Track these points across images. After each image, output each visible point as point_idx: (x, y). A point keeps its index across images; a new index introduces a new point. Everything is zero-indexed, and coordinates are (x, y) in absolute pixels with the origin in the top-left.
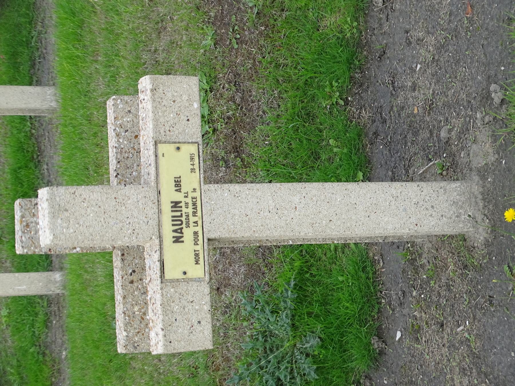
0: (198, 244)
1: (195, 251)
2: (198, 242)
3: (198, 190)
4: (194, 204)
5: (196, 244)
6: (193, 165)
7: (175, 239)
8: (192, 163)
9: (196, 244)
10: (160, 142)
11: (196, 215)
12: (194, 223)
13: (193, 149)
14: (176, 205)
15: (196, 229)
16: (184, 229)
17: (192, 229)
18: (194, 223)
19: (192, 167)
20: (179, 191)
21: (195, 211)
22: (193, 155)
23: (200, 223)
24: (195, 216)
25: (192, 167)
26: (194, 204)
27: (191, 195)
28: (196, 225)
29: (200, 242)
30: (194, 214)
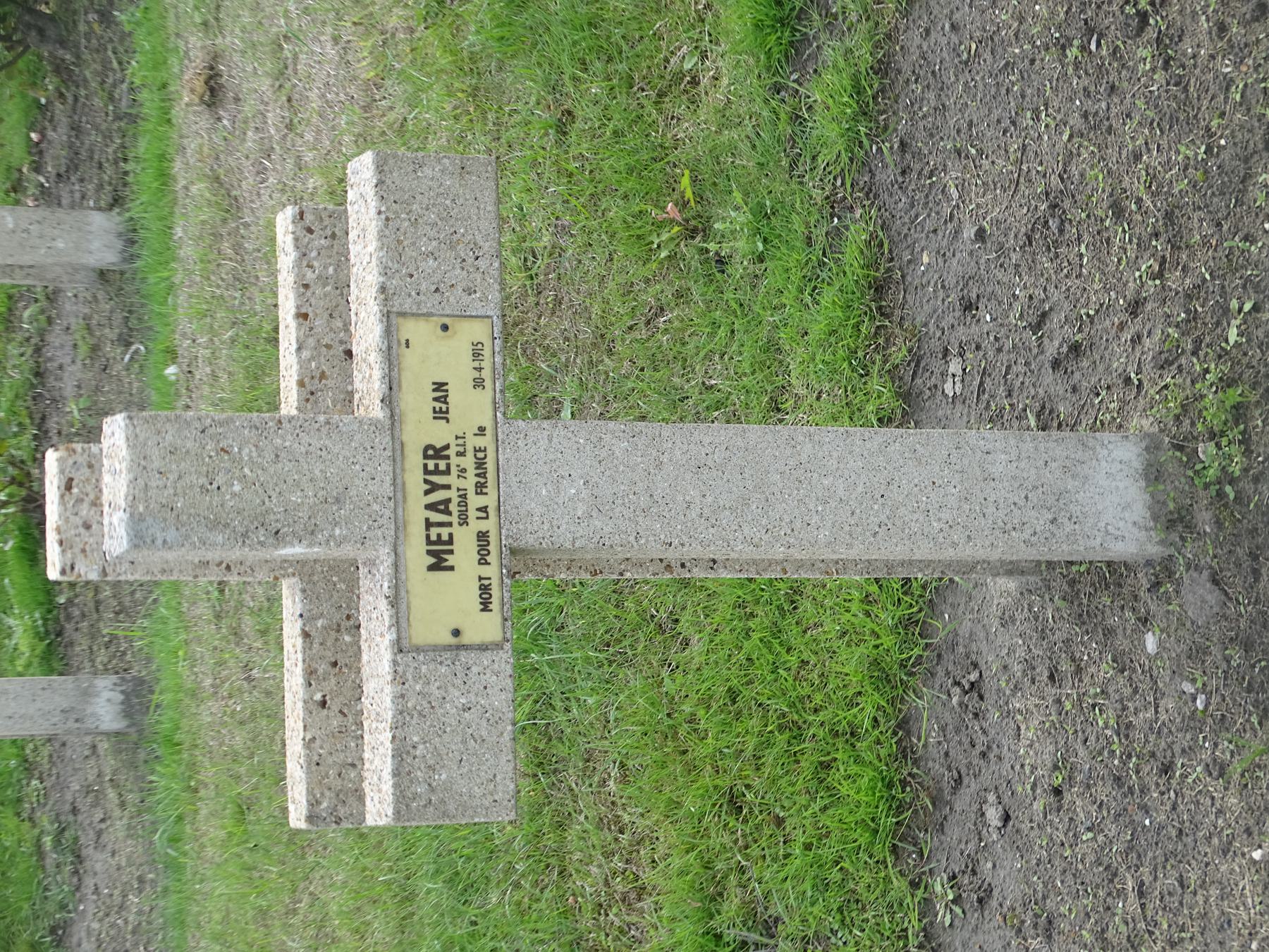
0: (487, 563)
1: (480, 578)
4: (480, 464)
8: (476, 364)
9: (483, 561)
10: (403, 314)
11: (485, 490)
12: (478, 509)
15: (483, 526)
16: (455, 524)
17: (476, 525)
18: (478, 509)
19: (477, 375)
21: (483, 480)
22: (480, 346)
23: (492, 511)
24: (482, 493)
25: (477, 375)
26: (480, 464)
27: (473, 442)
28: (484, 515)
30: (480, 488)
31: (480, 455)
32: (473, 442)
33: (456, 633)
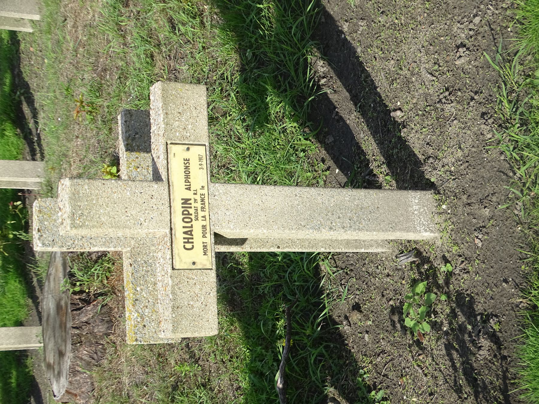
1: (203, 243)
3: (206, 188)
4: (203, 200)
6: (201, 165)
8: (200, 163)
9: (204, 236)
12: (202, 217)
13: (201, 151)
14: (186, 201)
15: (204, 223)
16: (194, 223)
18: (202, 217)
19: (201, 167)
20: (189, 189)
25: (201, 167)
26: (203, 200)
27: (200, 192)
30: (203, 209)
31: (203, 197)
32: (200, 192)
33: (194, 263)
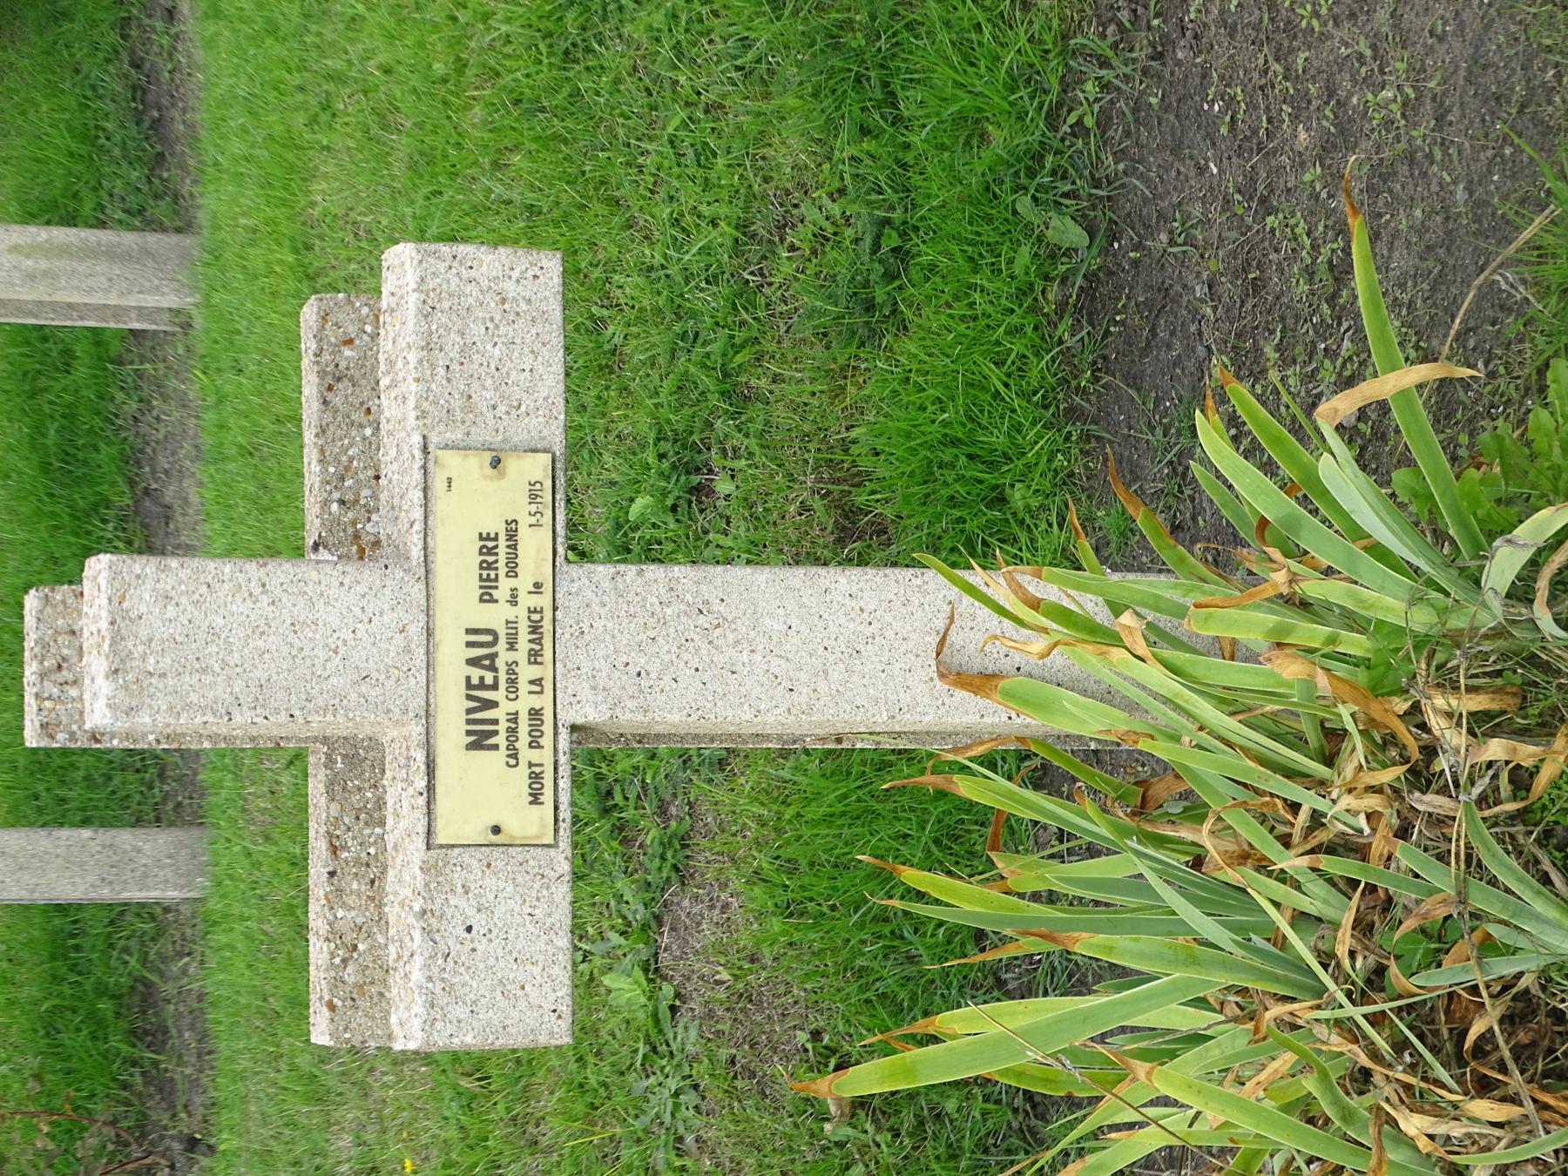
2: (542, 741)
3: (548, 587)
5: (534, 744)
7: (472, 738)
8: (533, 508)
9: (534, 744)
12: (532, 682)
15: (536, 702)
18: (532, 682)
19: (533, 520)
21: (537, 647)
24: (536, 662)
26: (535, 628)
28: (538, 689)
29: (547, 741)
30: (534, 657)
31: (536, 617)
